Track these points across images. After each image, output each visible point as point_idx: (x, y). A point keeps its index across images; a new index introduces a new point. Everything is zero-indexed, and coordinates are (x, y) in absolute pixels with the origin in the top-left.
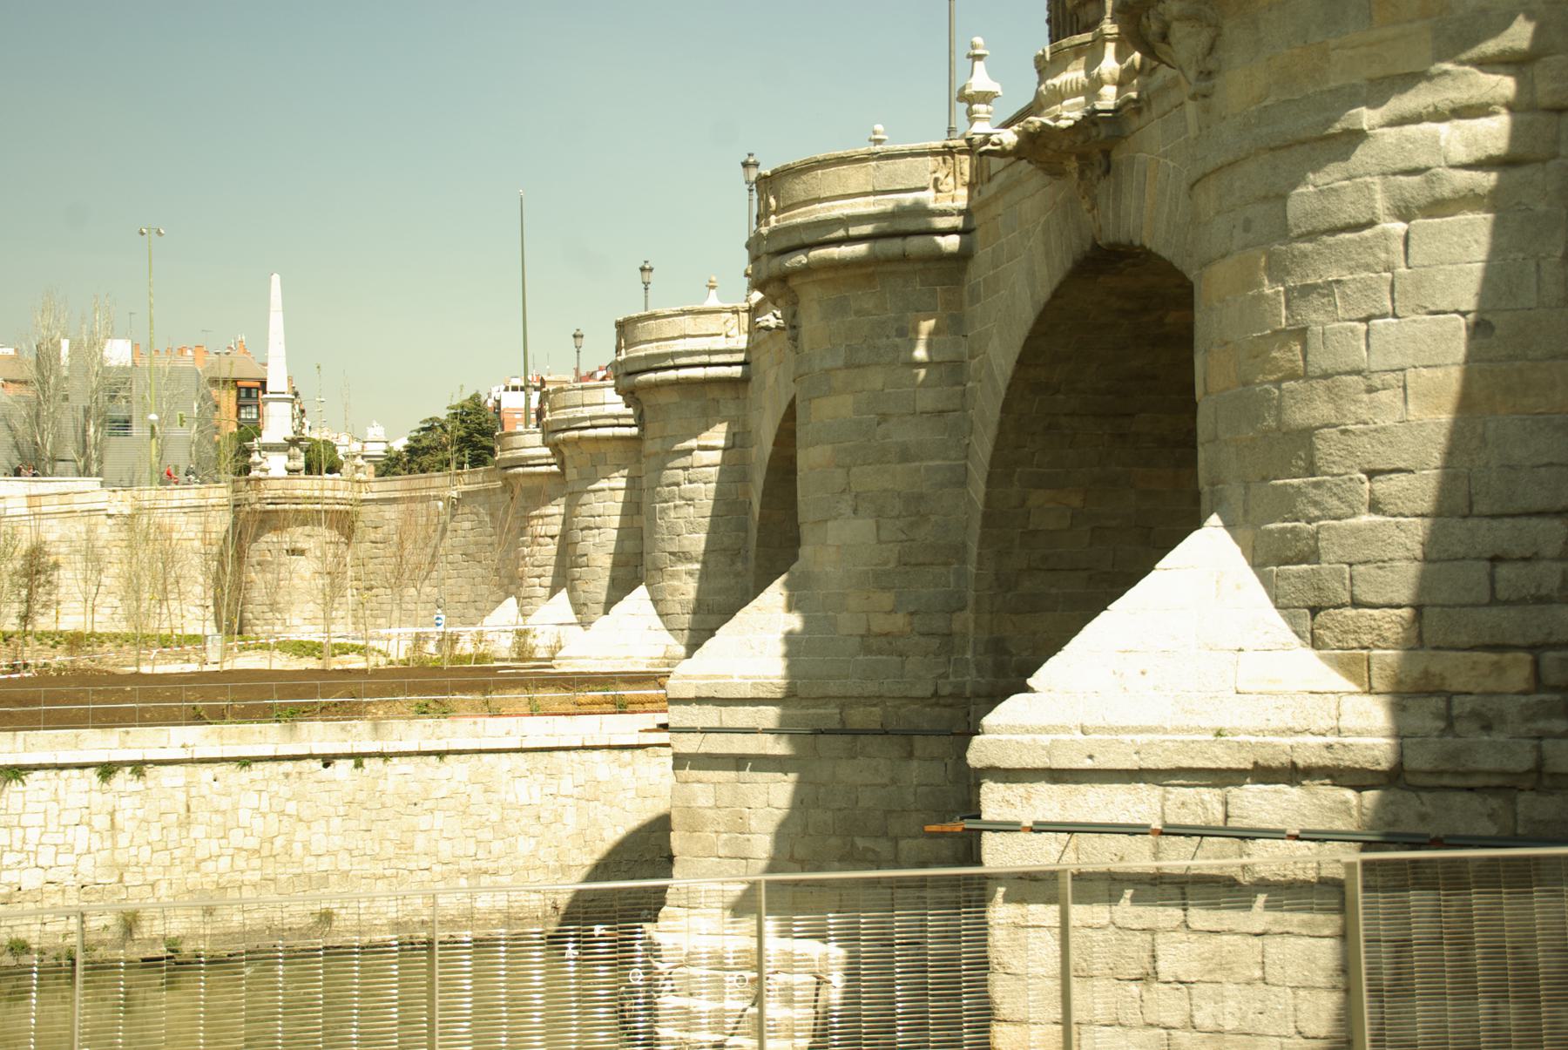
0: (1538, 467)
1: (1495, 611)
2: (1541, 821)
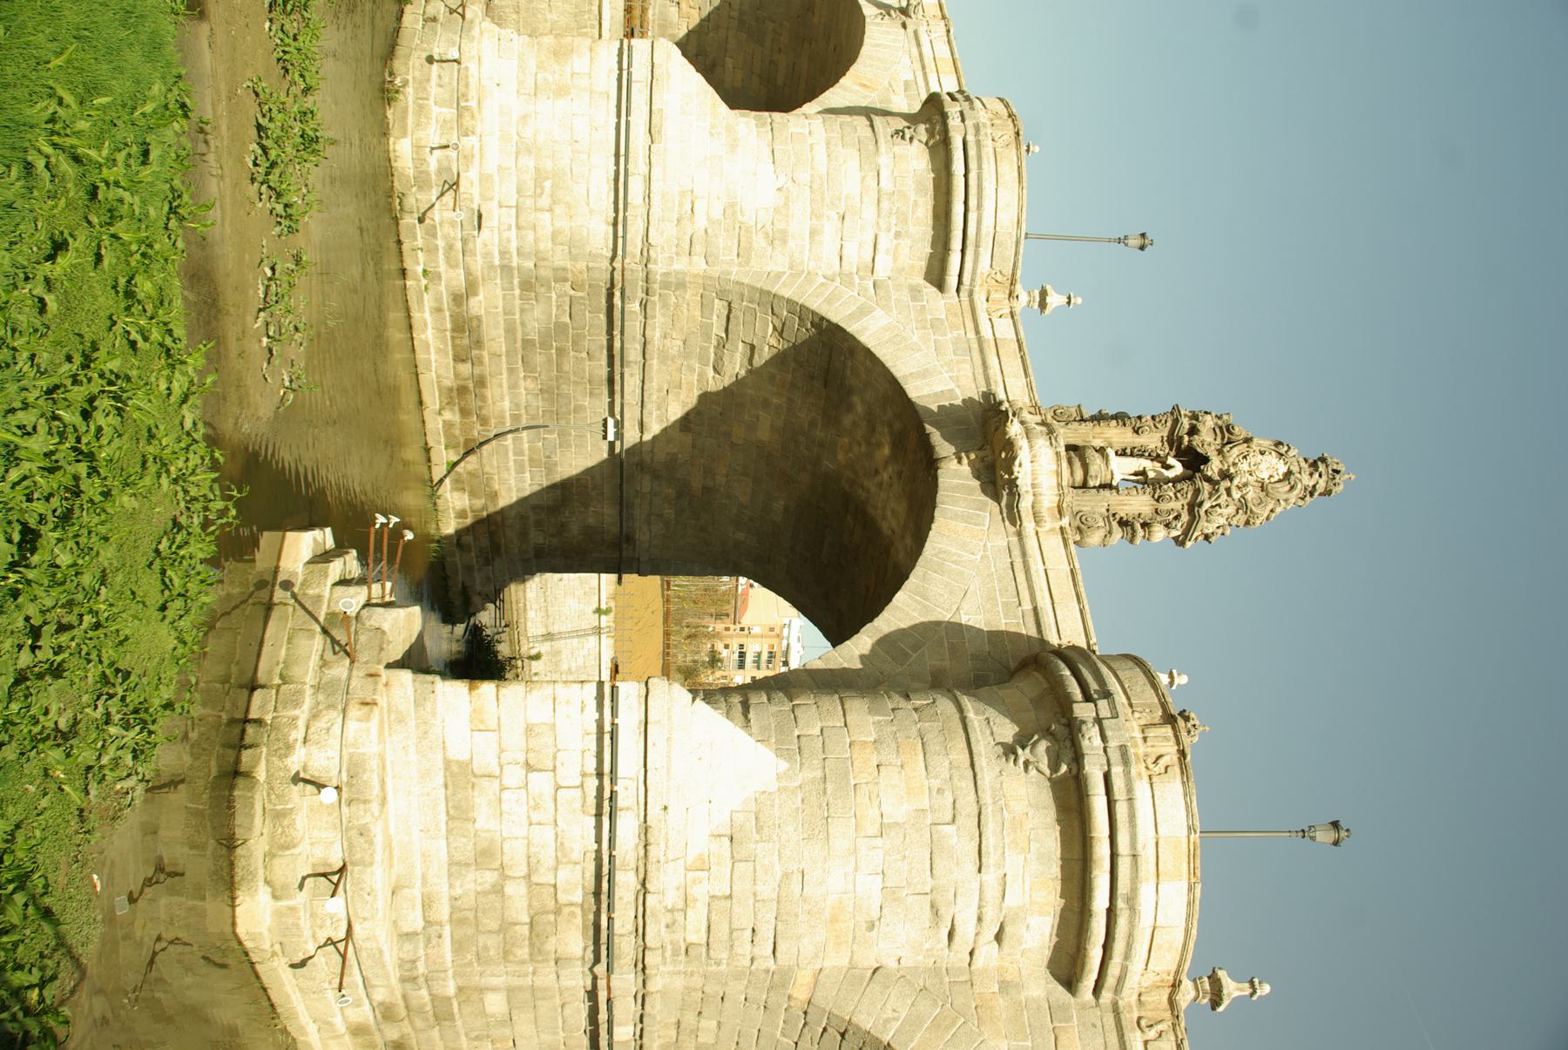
1: (727, 930)
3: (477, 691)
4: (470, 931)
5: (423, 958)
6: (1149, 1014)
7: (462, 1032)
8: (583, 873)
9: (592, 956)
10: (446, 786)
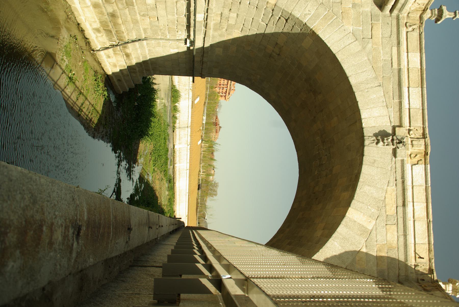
6: (411, 21)
7: (137, 12)
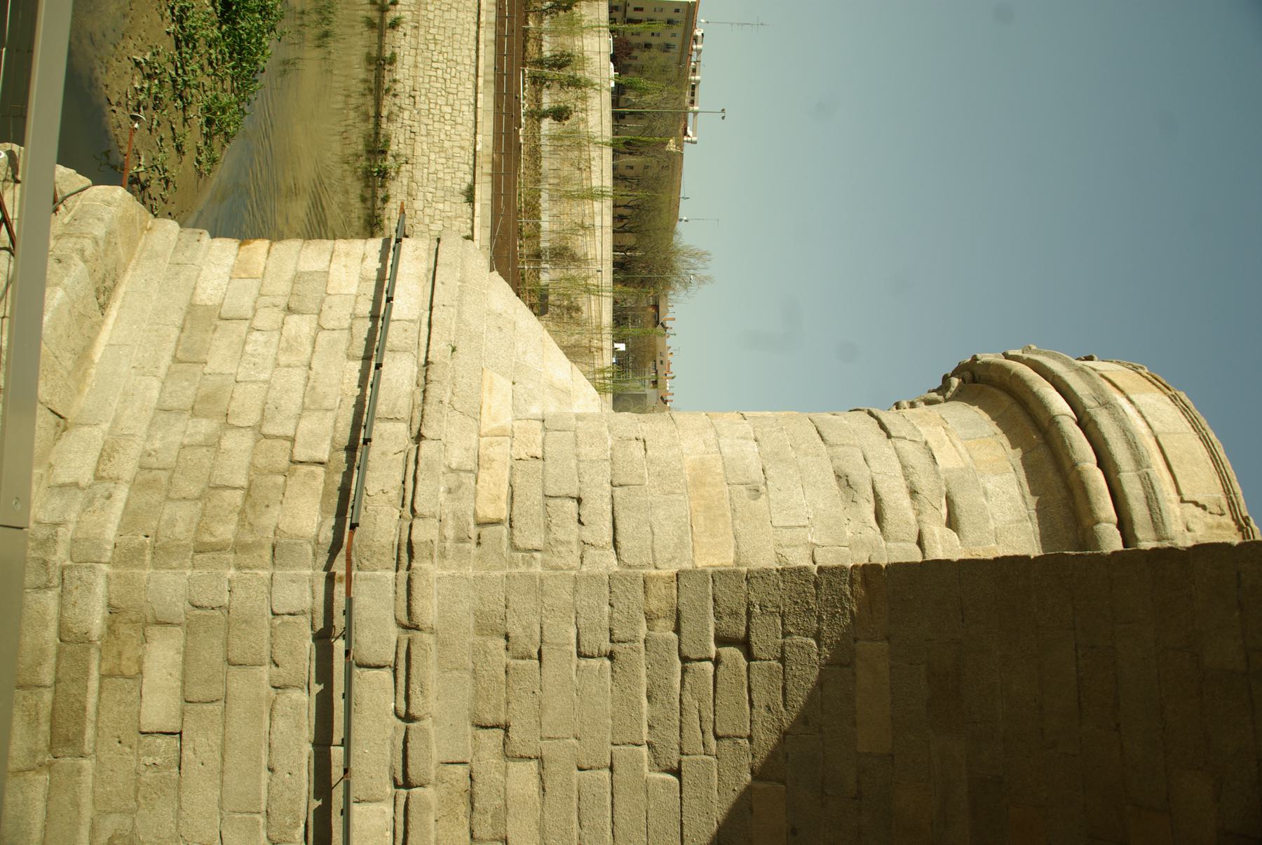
0: (651, 527)
1: (540, 497)
2: (376, 519)
3: (247, 246)
4: (156, 497)
5: (71, 527)
8: (336, 422)
9: (330, 534)
10: (182, 330)
